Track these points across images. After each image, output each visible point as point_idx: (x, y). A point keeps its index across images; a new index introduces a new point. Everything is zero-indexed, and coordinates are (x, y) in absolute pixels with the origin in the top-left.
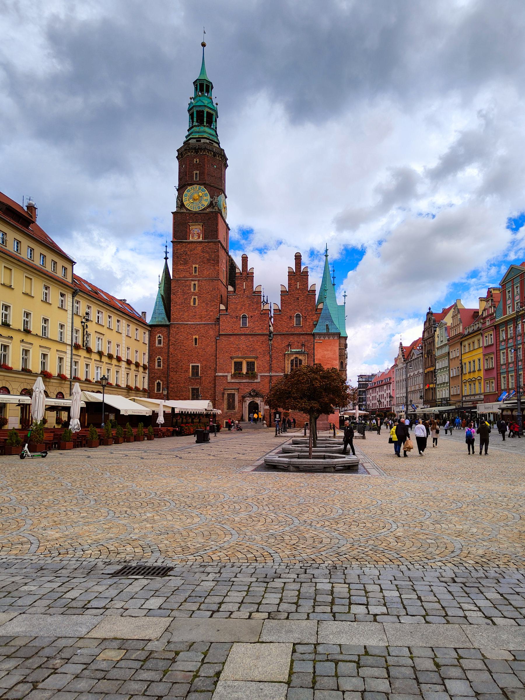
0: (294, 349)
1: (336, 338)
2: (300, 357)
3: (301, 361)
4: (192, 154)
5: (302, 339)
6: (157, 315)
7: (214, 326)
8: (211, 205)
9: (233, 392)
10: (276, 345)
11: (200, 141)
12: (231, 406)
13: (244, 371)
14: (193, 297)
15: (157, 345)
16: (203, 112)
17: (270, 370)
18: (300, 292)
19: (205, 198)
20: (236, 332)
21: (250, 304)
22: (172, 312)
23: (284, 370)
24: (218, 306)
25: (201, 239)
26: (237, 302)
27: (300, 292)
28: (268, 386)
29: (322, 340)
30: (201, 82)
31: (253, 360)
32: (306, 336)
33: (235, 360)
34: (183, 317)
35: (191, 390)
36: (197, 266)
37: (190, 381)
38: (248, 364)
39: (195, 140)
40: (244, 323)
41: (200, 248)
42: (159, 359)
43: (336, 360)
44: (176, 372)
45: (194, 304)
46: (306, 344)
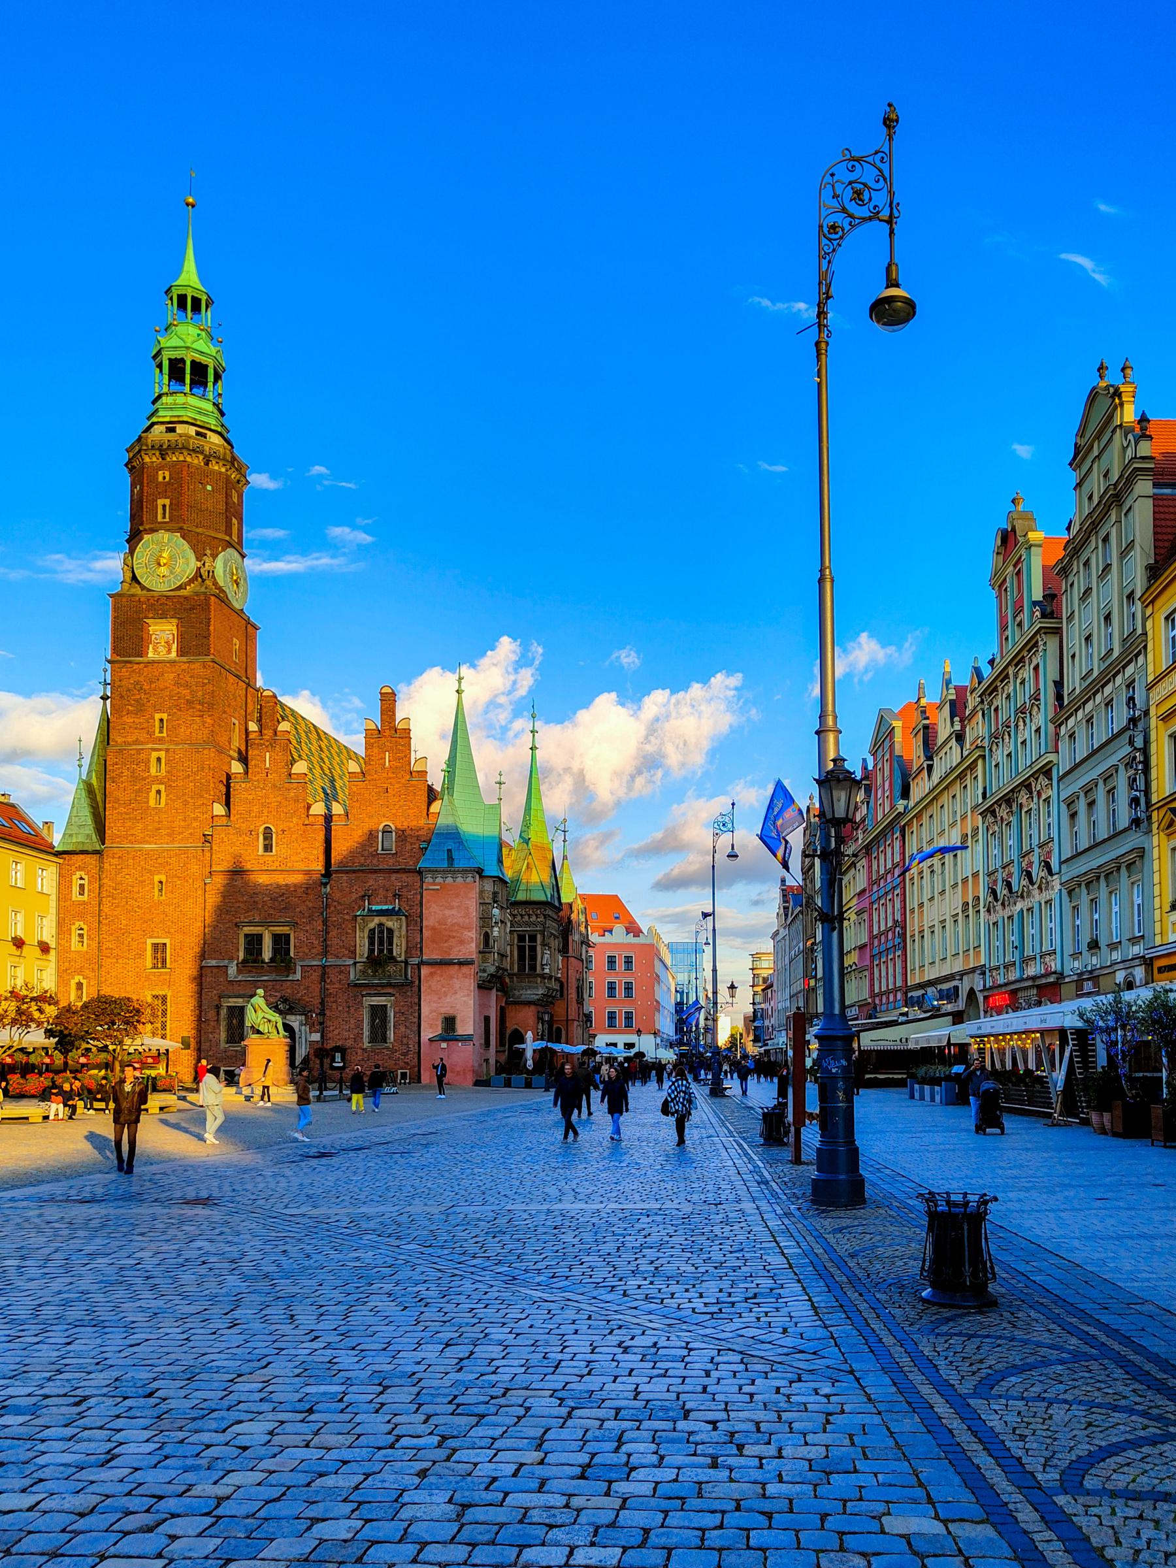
0: (378, 904)
1: (470, 879)
2: (390, 924)
3: (390, 931)
5: (396, 881)
6: (74, 830)
7: (200, 853)
10: (337, 895)
11: (173, 430)
13: (267, 955)
14: (155, 788)
15: (75, 895)
16: (183, 361)
17: (325, 953)
18: (390, 775)
23: (353, 953)
25: (174, 654)
26: (250, 797)
27: (390, 775)
28: (318, 990)
29: (439, 884)
32: (404, 876)
33: (247, 930)
34: (132, 832)
36: (165, 716)
39: (163, 428)
40: (268, 848)
41: (172, 676)
43: (469, 929)
44: (117, 957)
46: (404, 892)
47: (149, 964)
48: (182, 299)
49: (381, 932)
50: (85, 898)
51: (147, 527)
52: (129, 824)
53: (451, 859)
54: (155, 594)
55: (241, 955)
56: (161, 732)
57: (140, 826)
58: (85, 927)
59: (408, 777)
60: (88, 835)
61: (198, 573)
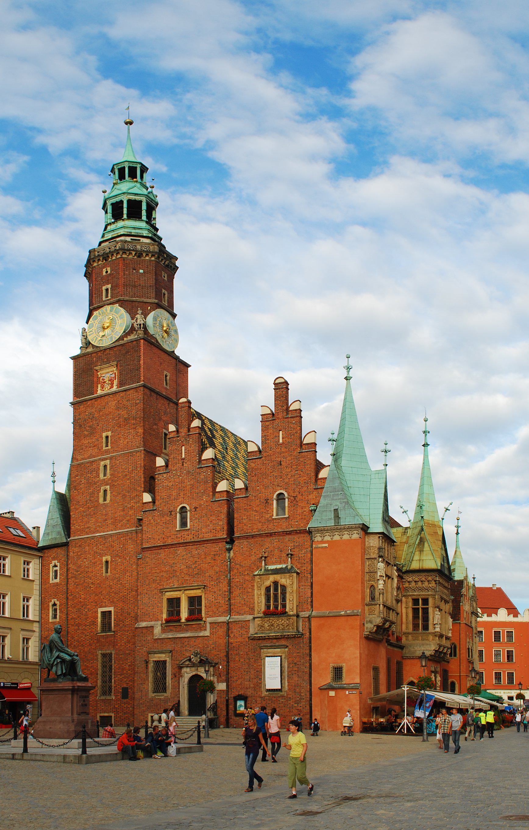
2: (283, 580)
3: (284, 587)
7: (134, 535)
8: (132, 330)
9: (162, 657)
12: (160, 685)
14: (102, 488)
17: (230, 611)
20: (169, 542)
22: (72, 519)
35: (100, 657)
36: (109, 434)
37: (98, 641)
41: (115, 402)
42: (55, 604)
45: (105, 500)
47: (99, 628)
49: (276, 589)
50: (58, 580)
52: (86, 519)
56: (107, 446)
57: (94, 520)
58: (58, 603)
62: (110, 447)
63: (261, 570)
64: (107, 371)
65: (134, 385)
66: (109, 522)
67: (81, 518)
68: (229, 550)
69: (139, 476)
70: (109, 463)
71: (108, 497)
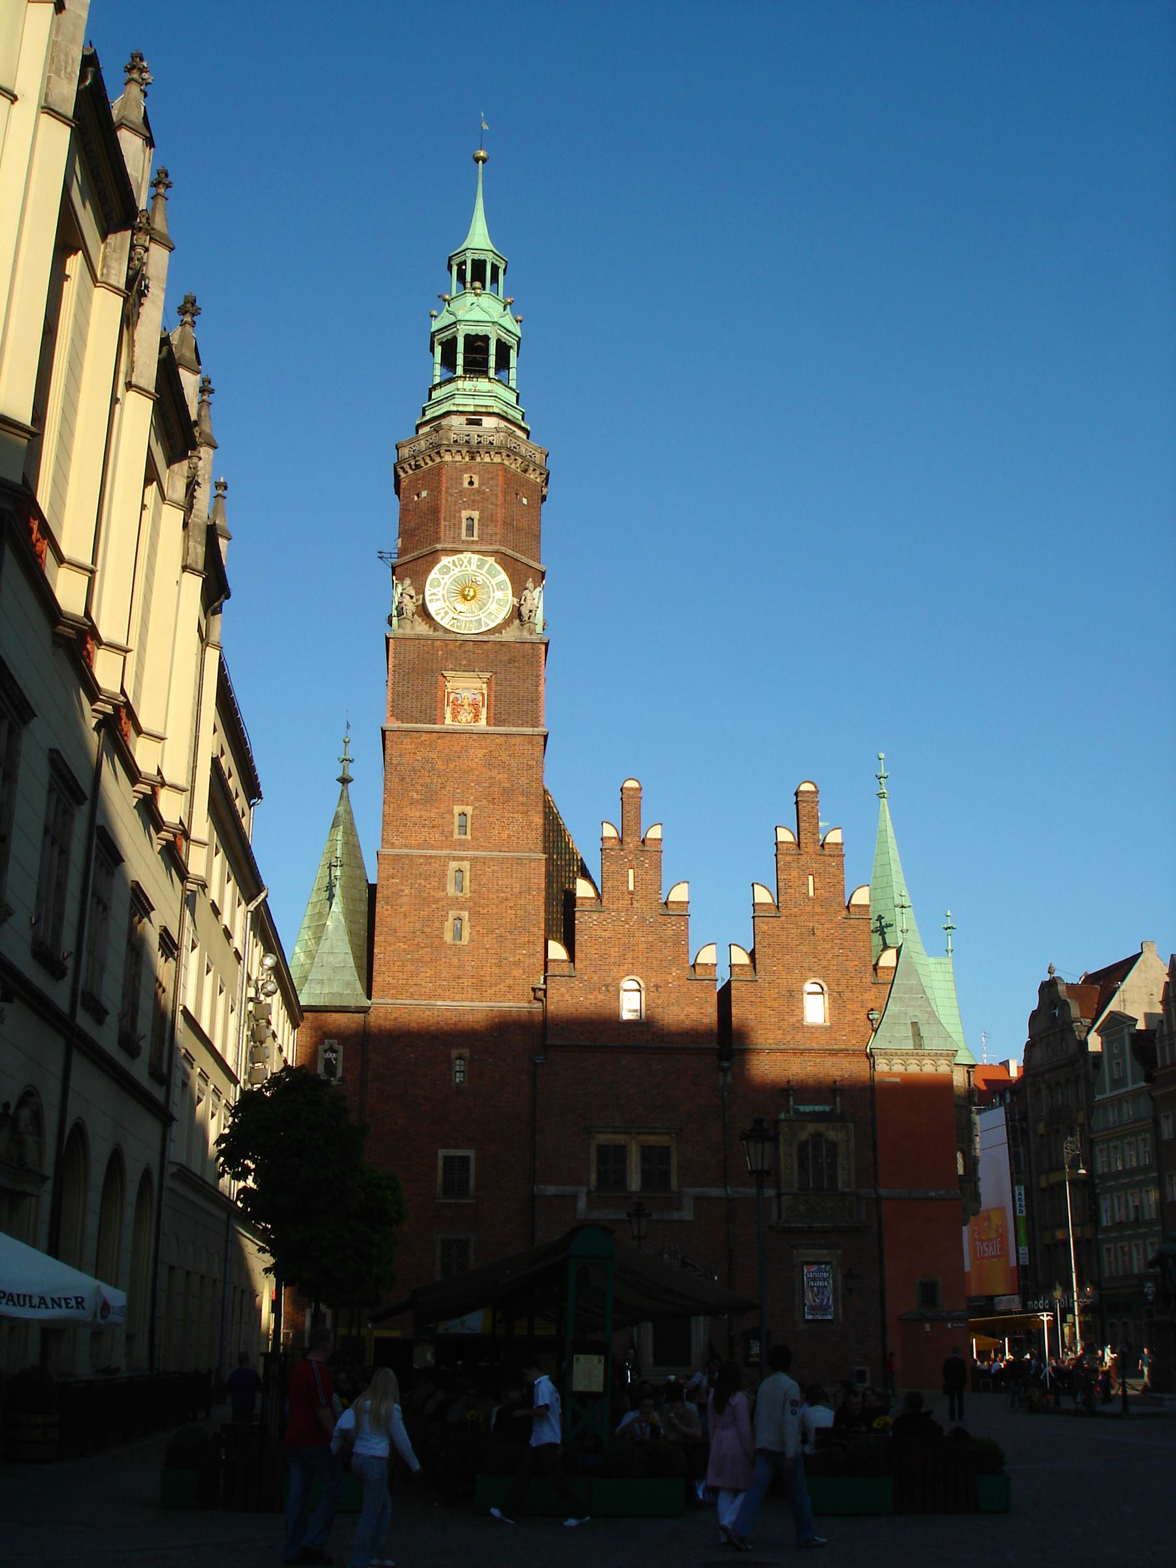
2: (831, 1134)
3: (833, 1146)
4: (458, 458)
11: (478, 423)
16: (486, 338)
18: (818, 910)
19: (499, 594)
21: (651, 947)
24: (540, 948)
26: (607, 934)
27: (818, 910)
30: (476, 257)
31: (663, 1140)
33: (603, 1138)
36: (469, 810)
38: (647, 1153)
41: (480, 753)
47: (439, 1188)
48: (479, 266)
51: (450, 546)
52: (409, 968)
53: (917, 1035)
54: (459, 637)
55: (593, 1177)
59: (844, 913)
60: (348, 984)
61: (517, 613)
62: (469, 837)
63: (788, 1111)
64: (466, 685)
65: (528, 730)
66: (467, 982)
67: (400, 963)
68: (724, 1071)
69: (535, 903)
70: (468, 867)
71: (466, 934)
